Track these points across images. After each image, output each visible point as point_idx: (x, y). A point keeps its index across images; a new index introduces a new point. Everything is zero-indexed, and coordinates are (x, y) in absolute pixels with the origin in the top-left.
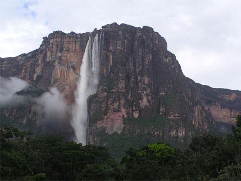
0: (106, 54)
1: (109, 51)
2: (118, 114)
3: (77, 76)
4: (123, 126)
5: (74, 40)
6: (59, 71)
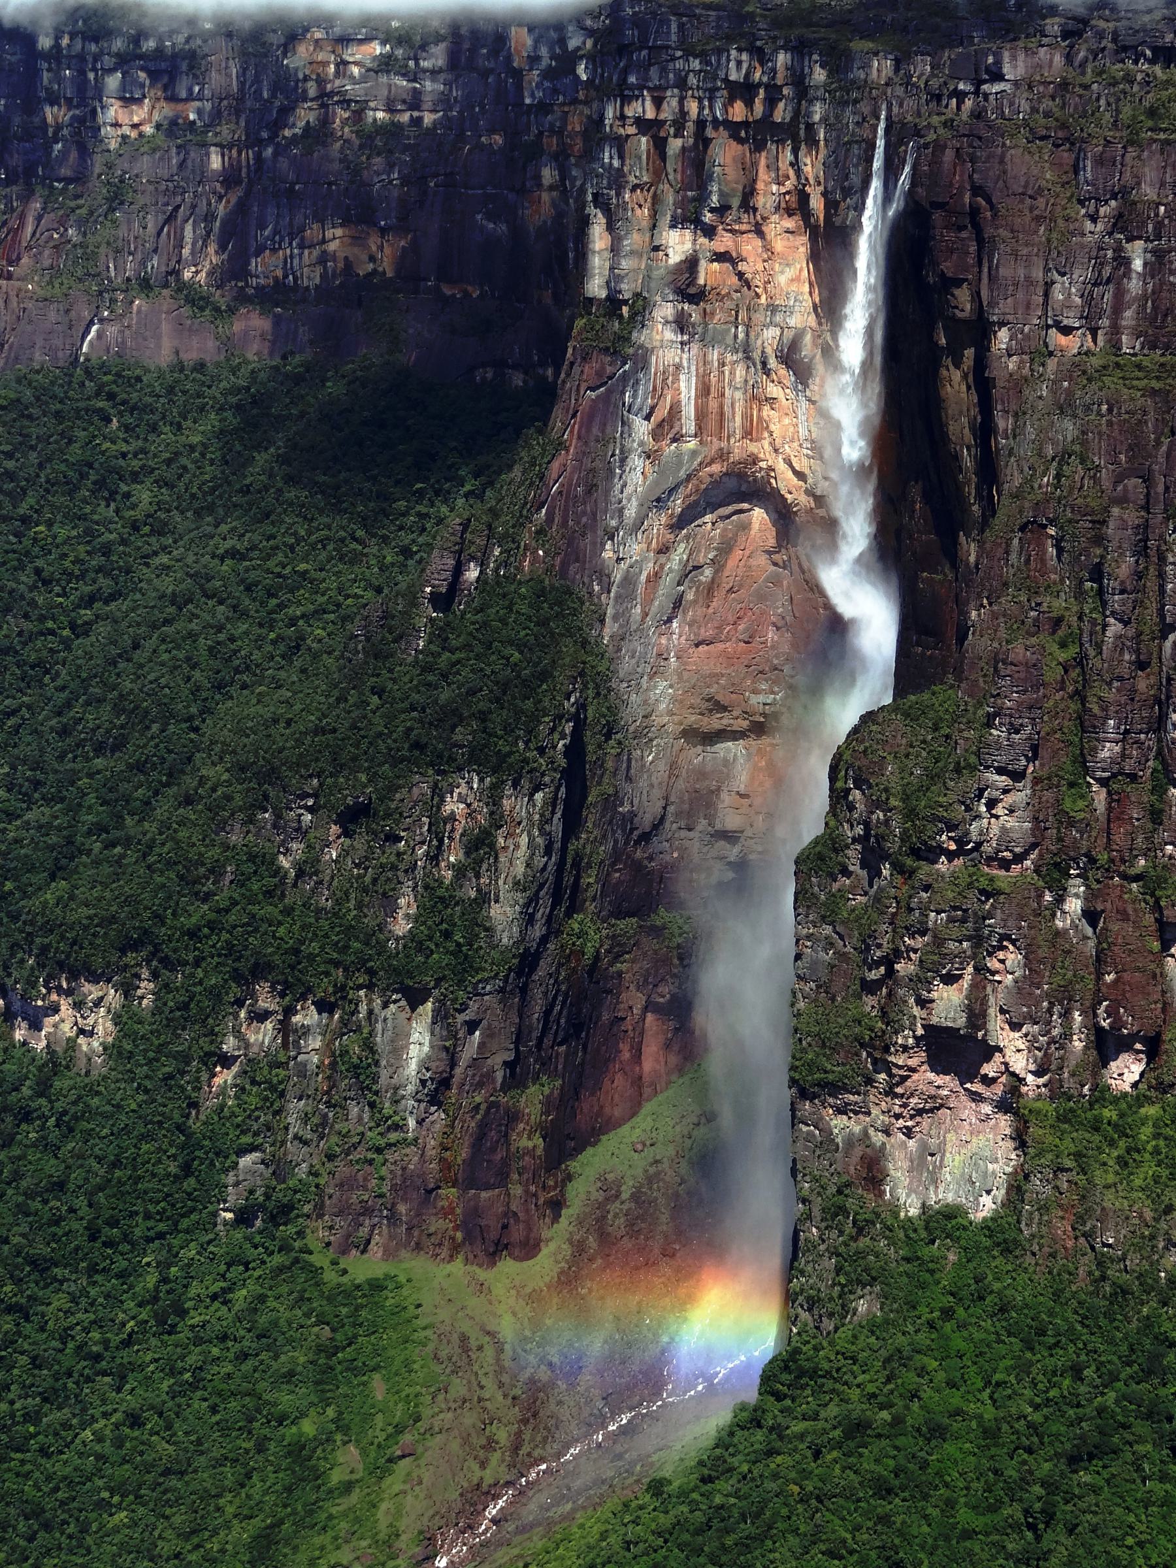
6: (687, 388)
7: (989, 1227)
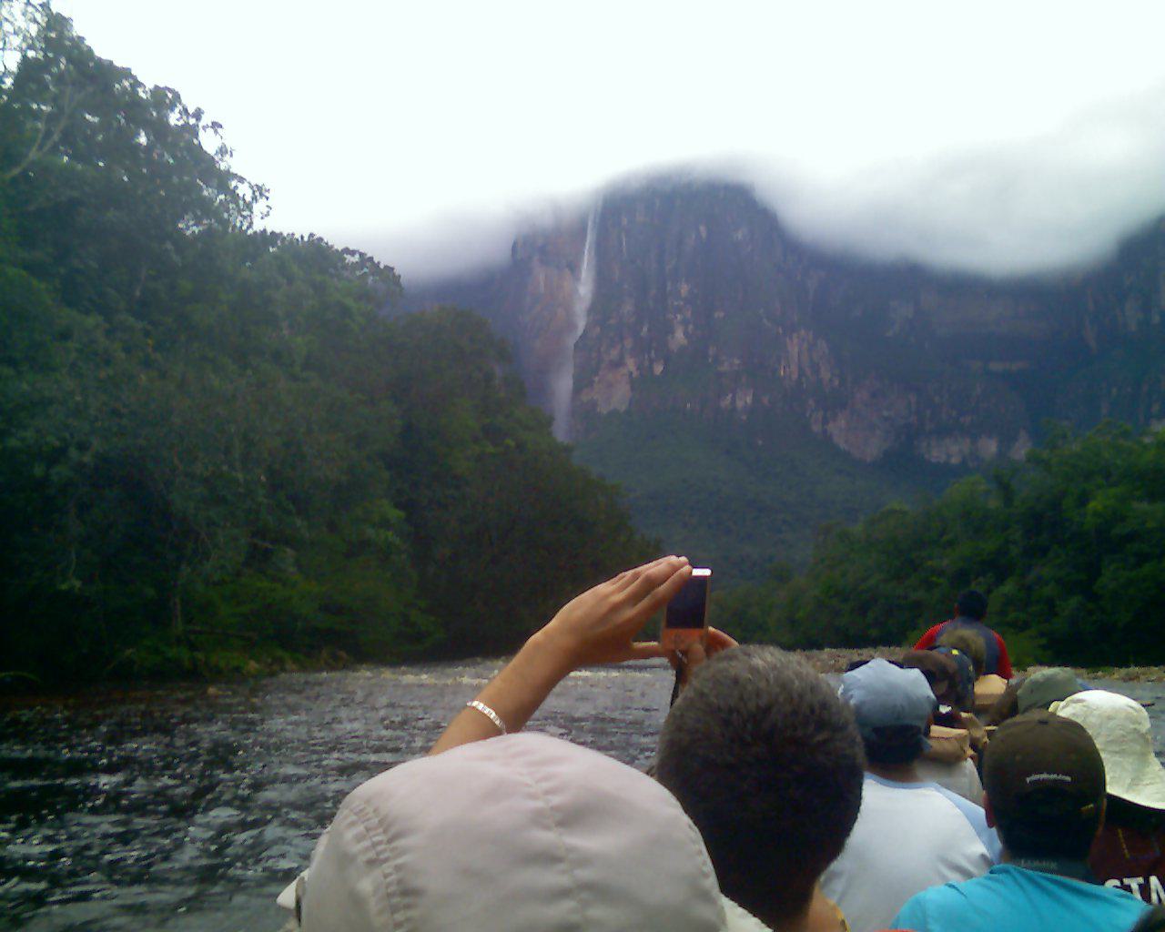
2: (624, 371)
6: (541, 277)
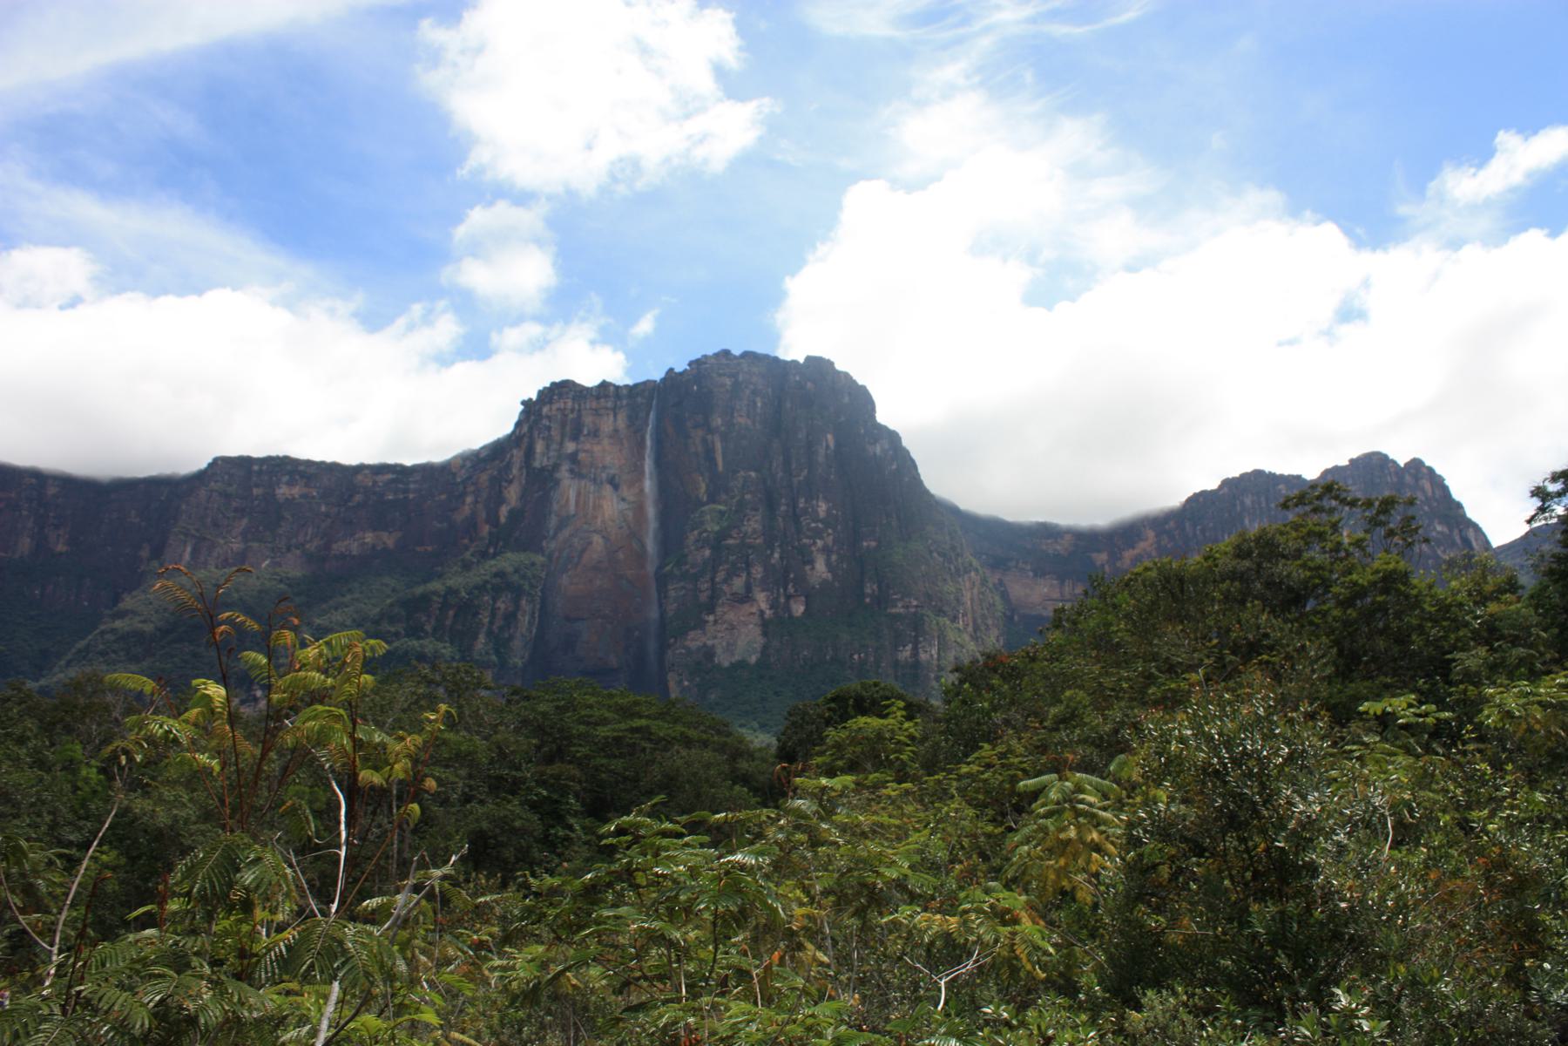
0: (704, 441)
1: (710, 431)
2: (747, 608)
3: (623, 506)
4: (760, 640)
5: (610, 405)
6: (572, 495)
7: (758, 663)
